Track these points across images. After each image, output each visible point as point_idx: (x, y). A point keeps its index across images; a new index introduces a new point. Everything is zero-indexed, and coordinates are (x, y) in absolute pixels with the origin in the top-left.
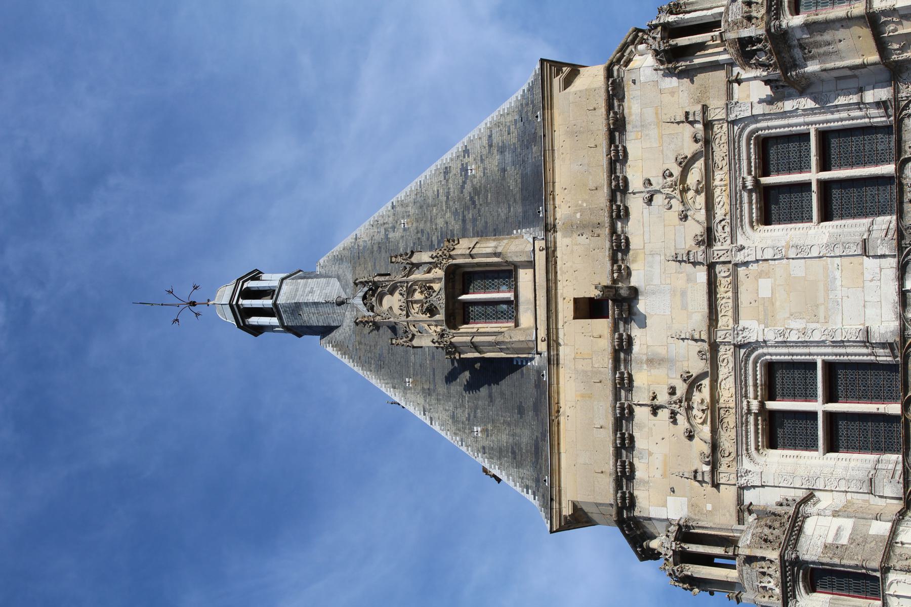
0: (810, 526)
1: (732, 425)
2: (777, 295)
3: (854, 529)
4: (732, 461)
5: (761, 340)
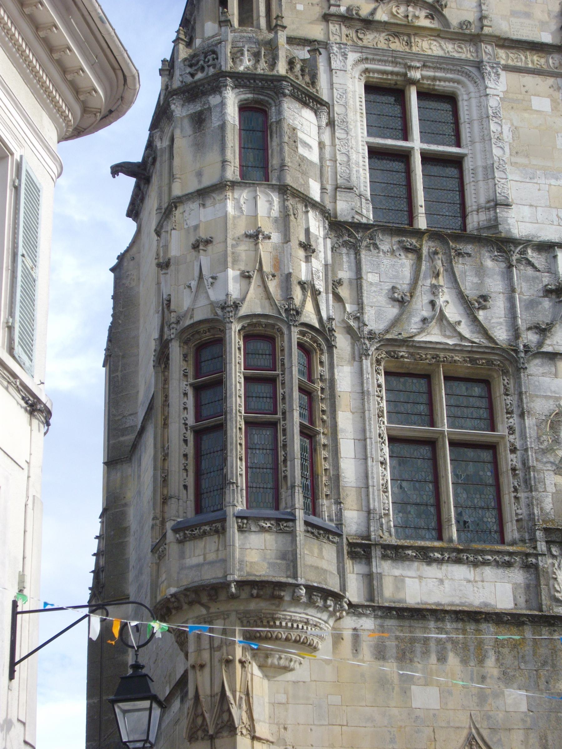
0: (308, 114)
1: (393, 46)
2: (535, 116)
3: (311, 162)
4: (353, 41)
5: (488, 91)
